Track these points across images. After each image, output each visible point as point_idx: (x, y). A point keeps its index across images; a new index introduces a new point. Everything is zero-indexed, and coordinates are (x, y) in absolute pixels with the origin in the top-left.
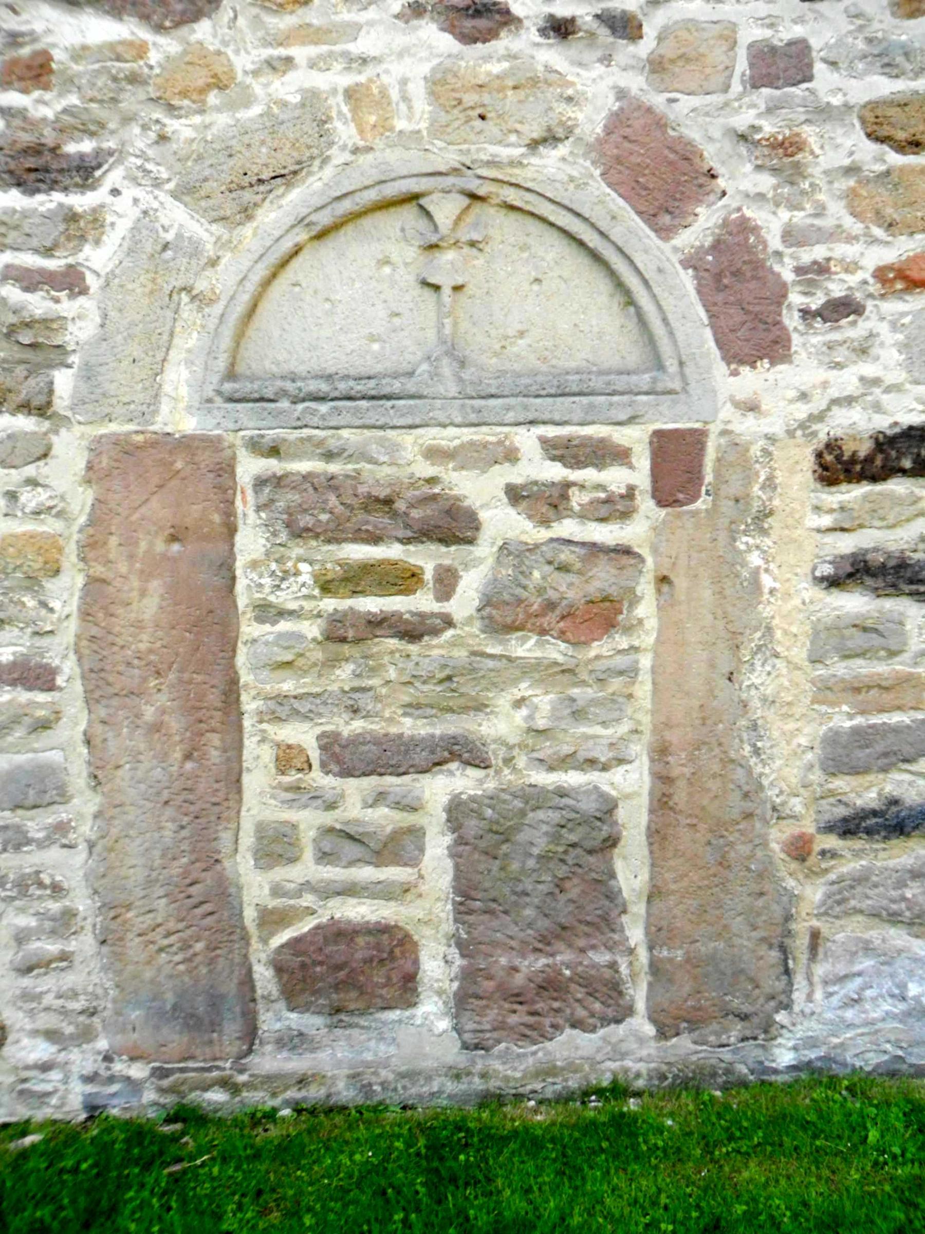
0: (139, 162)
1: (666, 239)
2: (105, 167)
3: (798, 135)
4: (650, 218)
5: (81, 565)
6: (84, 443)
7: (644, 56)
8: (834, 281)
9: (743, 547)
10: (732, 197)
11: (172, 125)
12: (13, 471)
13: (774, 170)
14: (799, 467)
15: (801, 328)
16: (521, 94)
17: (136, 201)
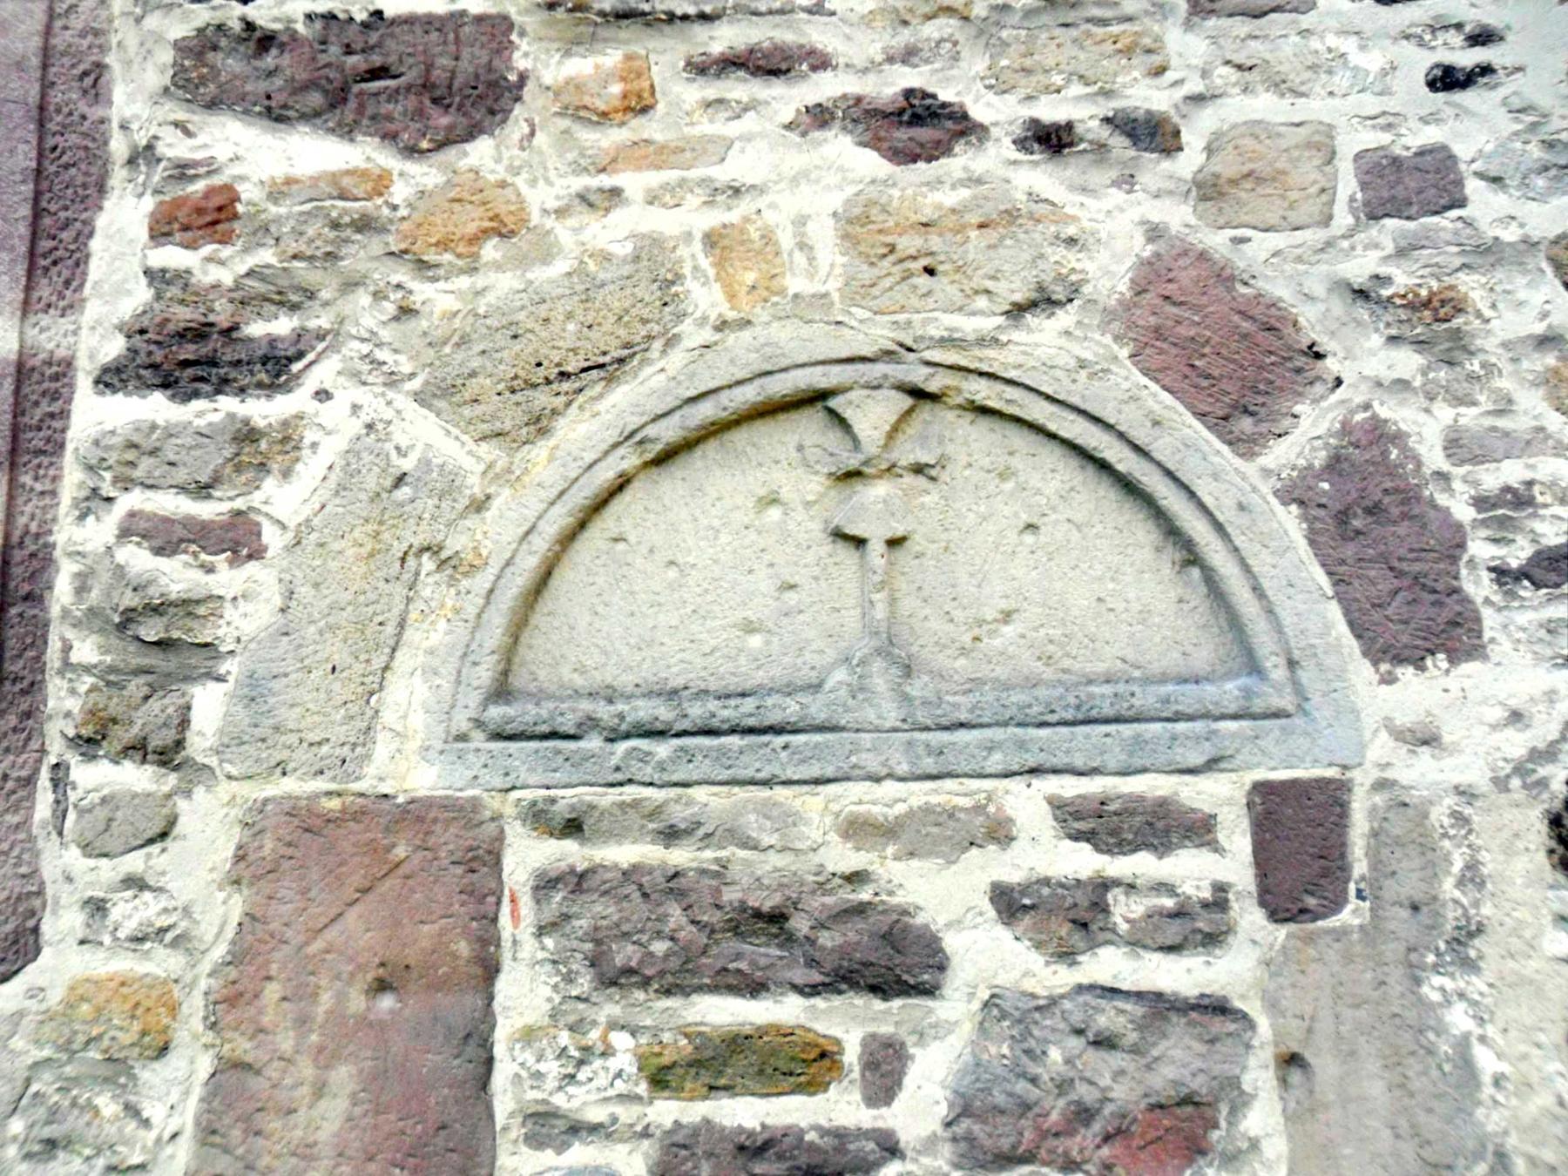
0: (365, 348)
1: (1249, 455)
2: (310, 357)
3: (1451, 288)
4: (1219, 423)
5: (209, 1037)
6: (236, 813)
7: (1189, 177)
8: (1543, 518)
9: (1435, 997)
10: (1354, 386)
11: (422, 291)
12: (104, 862)
13: (1420, 344)
14: (1520, 845)
15: (1496, 598)
16: (992, 235)
17: (356, 408)
